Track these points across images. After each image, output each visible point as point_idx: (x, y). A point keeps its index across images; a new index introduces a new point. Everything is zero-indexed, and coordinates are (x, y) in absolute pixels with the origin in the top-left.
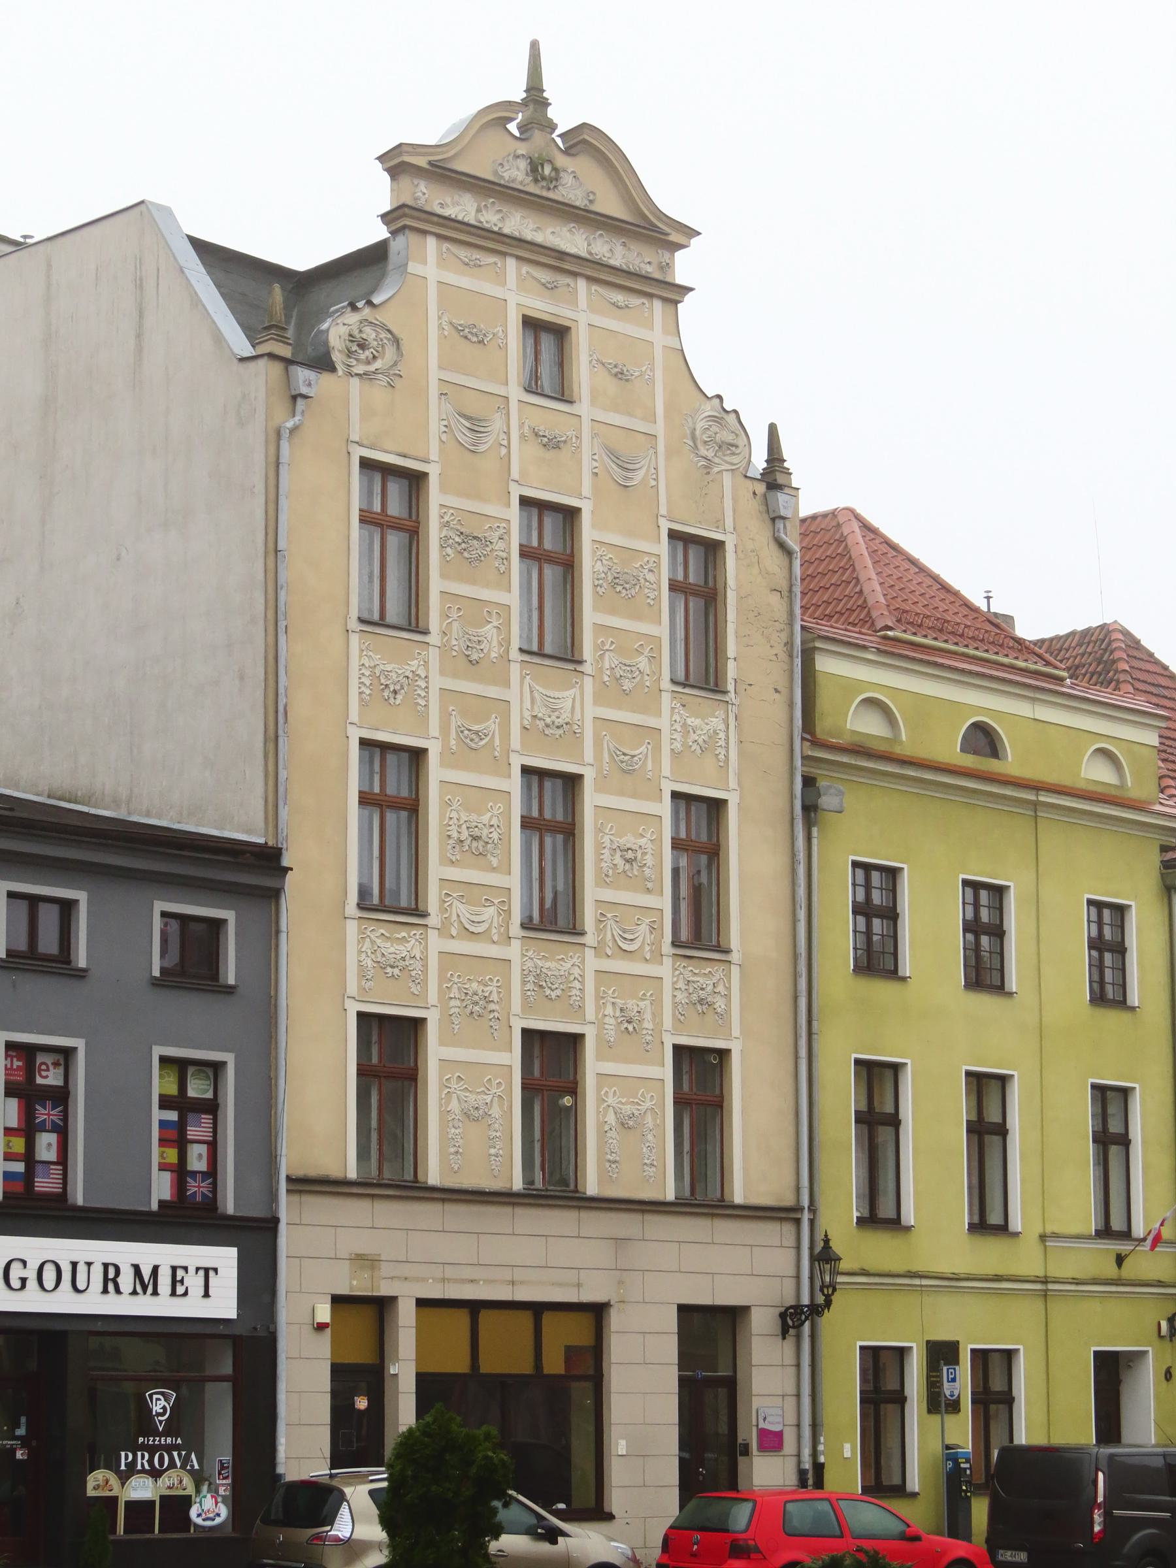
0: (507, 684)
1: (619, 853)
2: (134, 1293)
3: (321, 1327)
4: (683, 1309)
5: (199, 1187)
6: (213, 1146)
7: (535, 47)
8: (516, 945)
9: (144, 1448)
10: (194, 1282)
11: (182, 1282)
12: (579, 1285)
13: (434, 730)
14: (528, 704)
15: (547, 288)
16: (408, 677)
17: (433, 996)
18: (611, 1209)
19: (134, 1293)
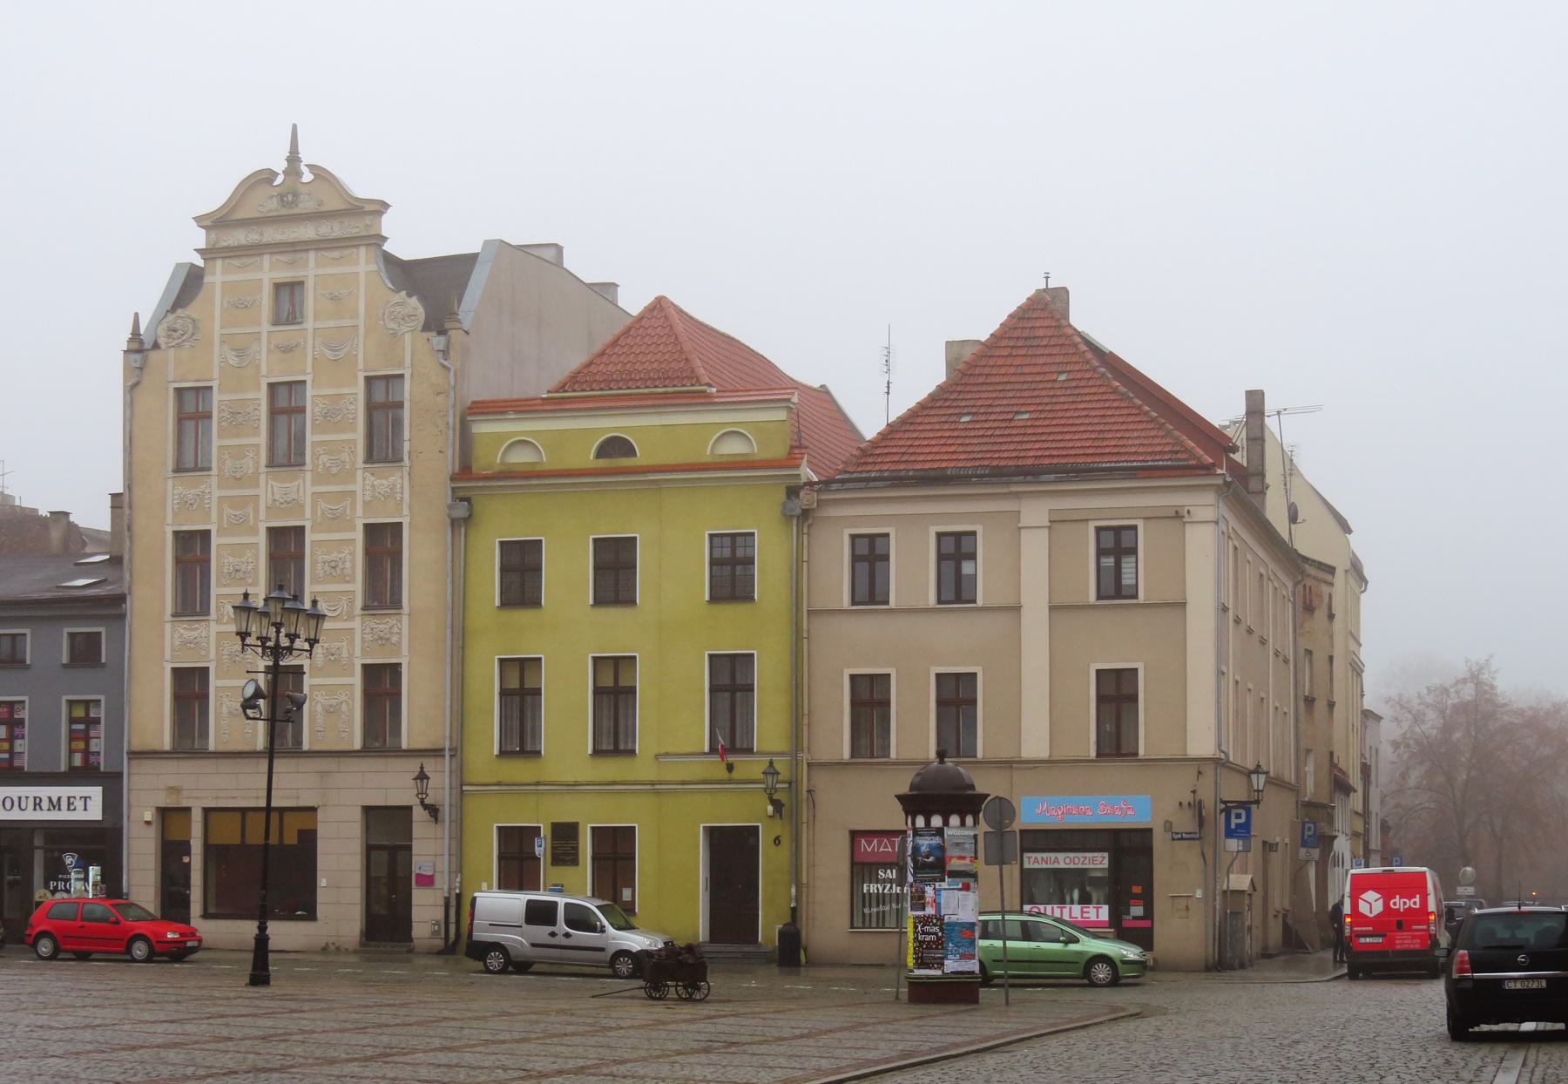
0: (257, 485)
2: (49, 810)
3: (148, 823)
4: (368, 811)
7: (295, 127)
9: (62, 880)
10: (79, 804)
11: (73, 804)
12: (298, 798)
14: (269, 495)
17: (212, 655)
18: (327, 756)
19: (49, 810)
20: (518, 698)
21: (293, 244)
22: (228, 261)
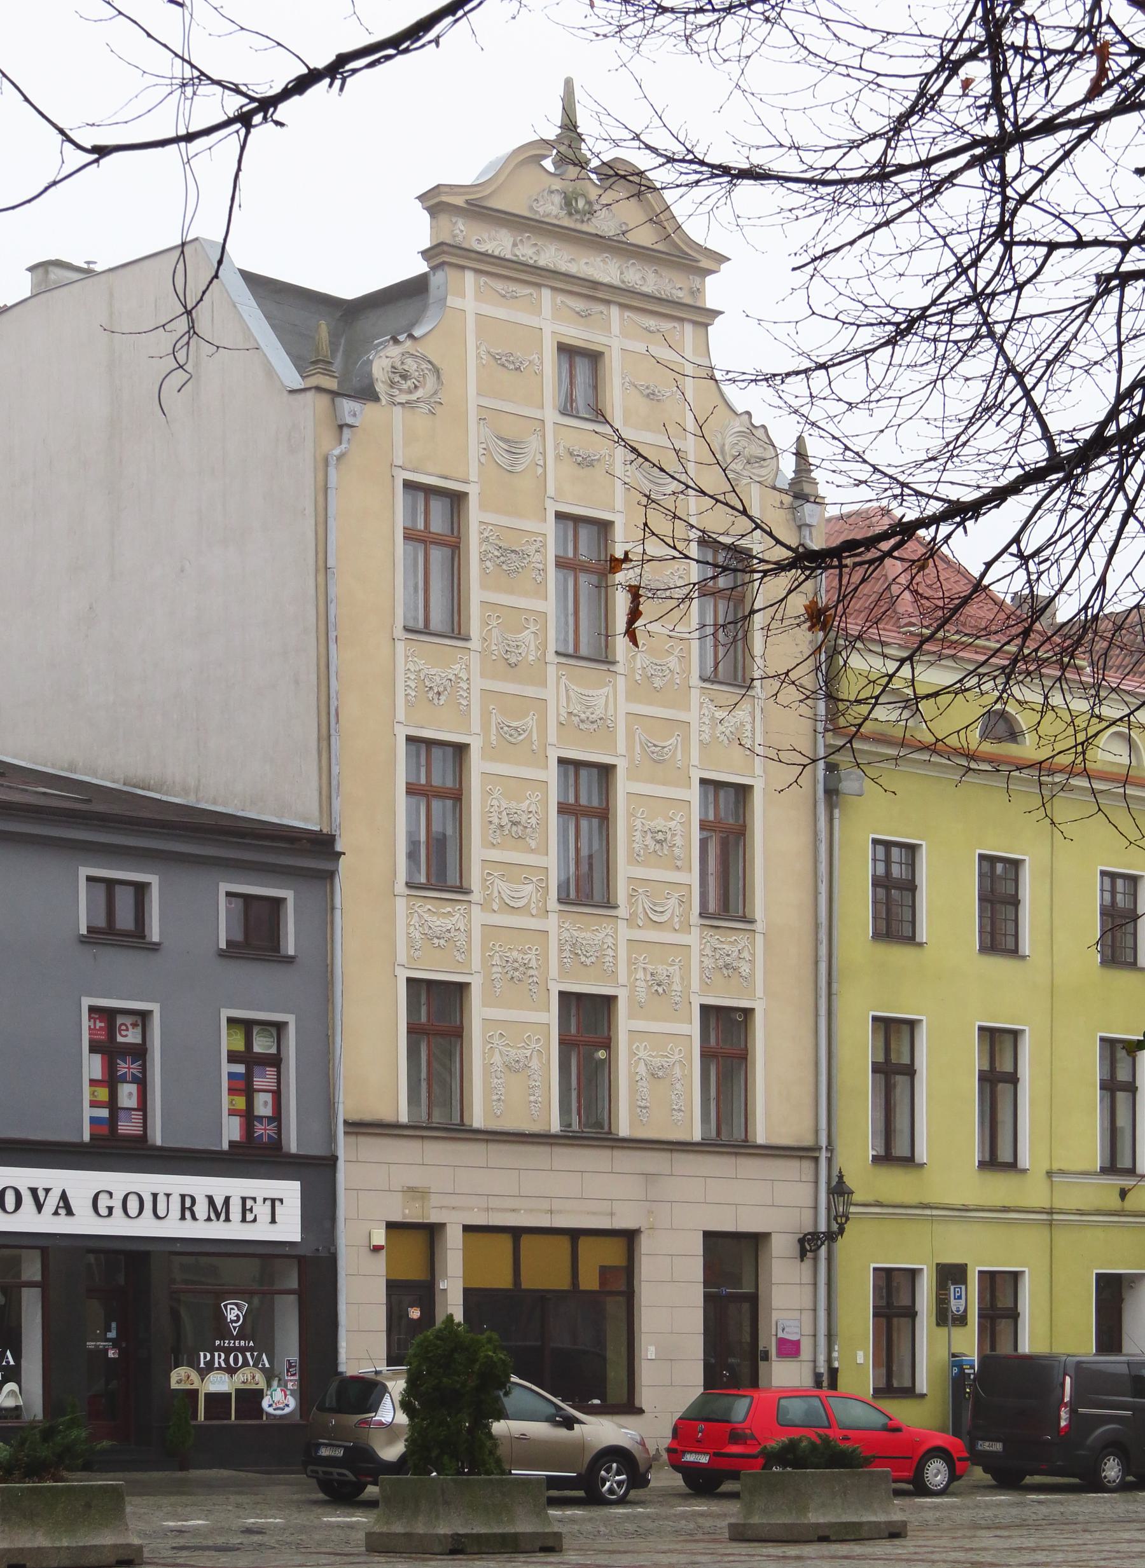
0: (544, 684)
2: (209, 1219)
3: (377, 1249)
5: (265, 1129)
6: (277, 1095)
8: (553, 918)
9: (220, 1349)
10: (262, 1211)
11: (251, 1210)
13: (476, 727)
15: (582, 316)
16: (451, 680)
17: (476, 964)
19: (209, 1219)
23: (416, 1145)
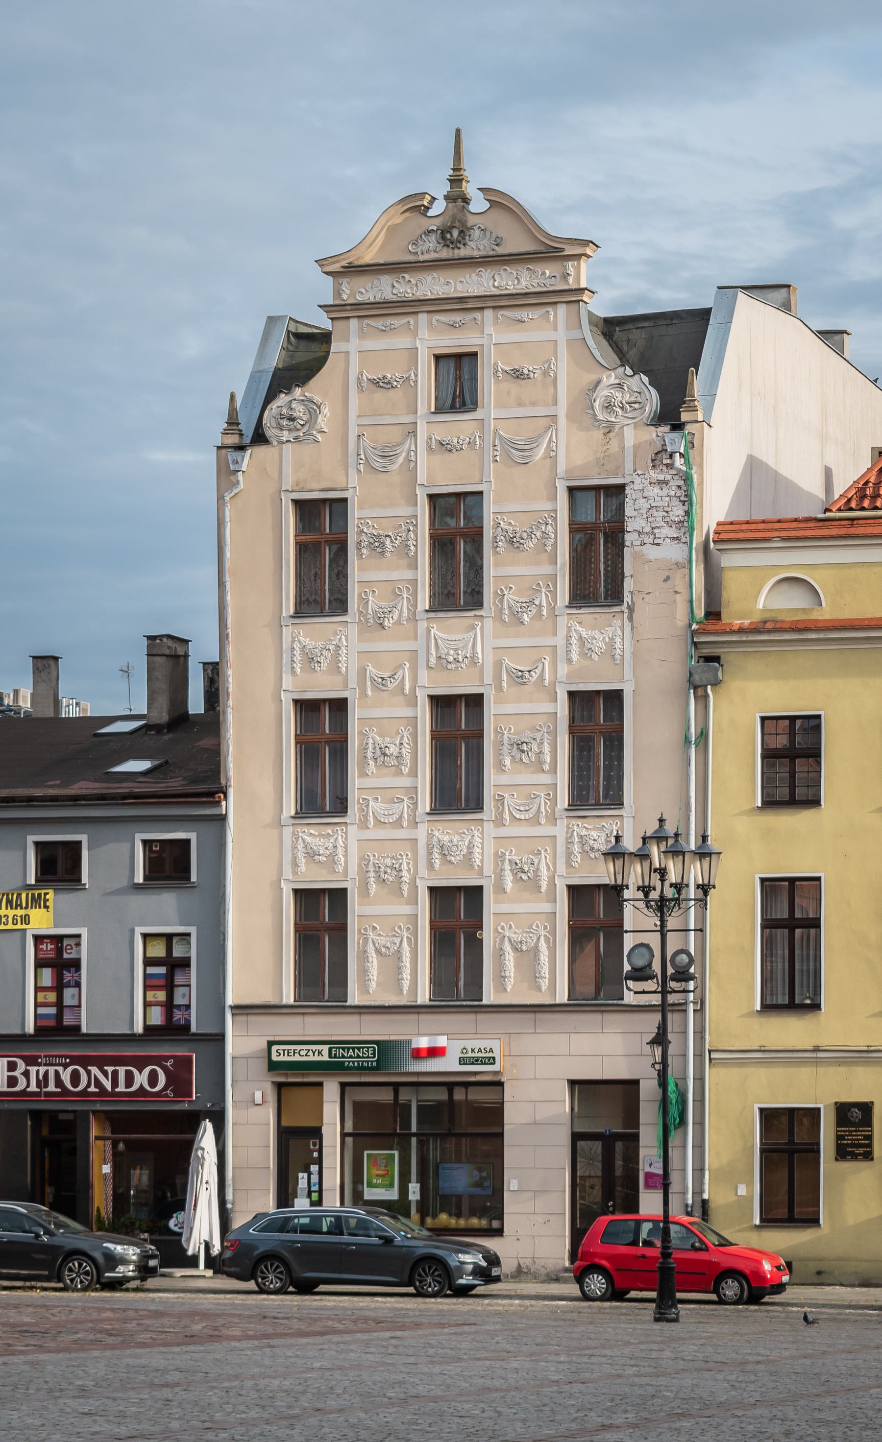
1: (515, 746)
20: (786, 931)
21: (461, 299)
22: (367, 321)
23: (298, 1019)
